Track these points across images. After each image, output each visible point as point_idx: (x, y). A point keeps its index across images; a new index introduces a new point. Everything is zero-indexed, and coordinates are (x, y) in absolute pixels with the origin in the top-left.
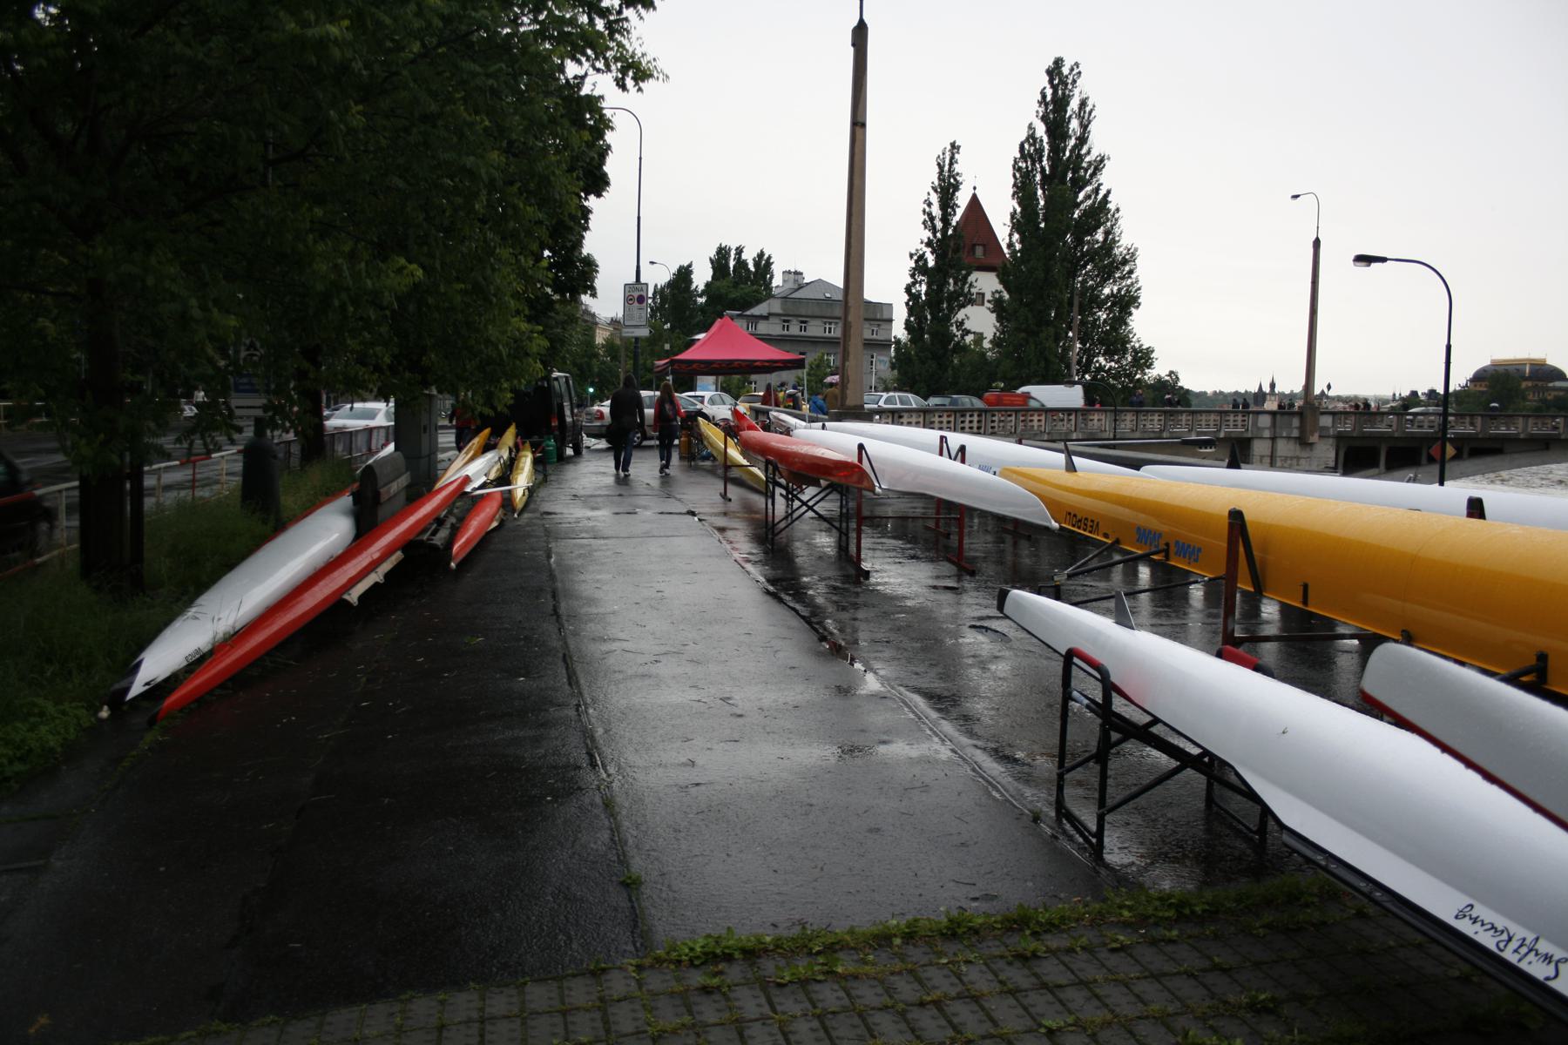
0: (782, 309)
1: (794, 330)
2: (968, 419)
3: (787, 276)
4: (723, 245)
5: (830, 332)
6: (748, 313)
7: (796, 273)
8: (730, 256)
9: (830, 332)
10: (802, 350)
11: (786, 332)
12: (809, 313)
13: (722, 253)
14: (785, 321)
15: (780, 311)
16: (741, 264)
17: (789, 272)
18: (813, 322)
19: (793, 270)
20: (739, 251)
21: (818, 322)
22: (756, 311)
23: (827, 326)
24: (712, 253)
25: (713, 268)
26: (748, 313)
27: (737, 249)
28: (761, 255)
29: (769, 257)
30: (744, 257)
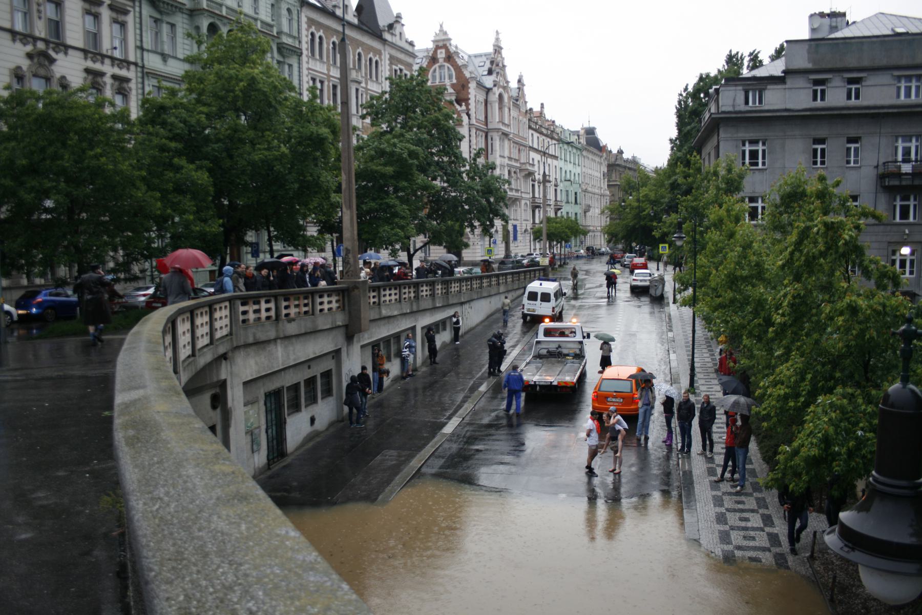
0: (810, 60)
1: (836, 96)
3: (818, 22)
4: (733, 53)
5: (908, 95)
7: (833, 15)
8: (742, 64)
9: (908, 95)
10: (853, 133)
11: (819, 103)
12: (866, 63)
14: (817, 82)
15: (809, 66)
17: (822, 15)
18: (872, 80)
19: (827, 11)
21: (885, 78)
23: (903, 85)
27: (751, 54)
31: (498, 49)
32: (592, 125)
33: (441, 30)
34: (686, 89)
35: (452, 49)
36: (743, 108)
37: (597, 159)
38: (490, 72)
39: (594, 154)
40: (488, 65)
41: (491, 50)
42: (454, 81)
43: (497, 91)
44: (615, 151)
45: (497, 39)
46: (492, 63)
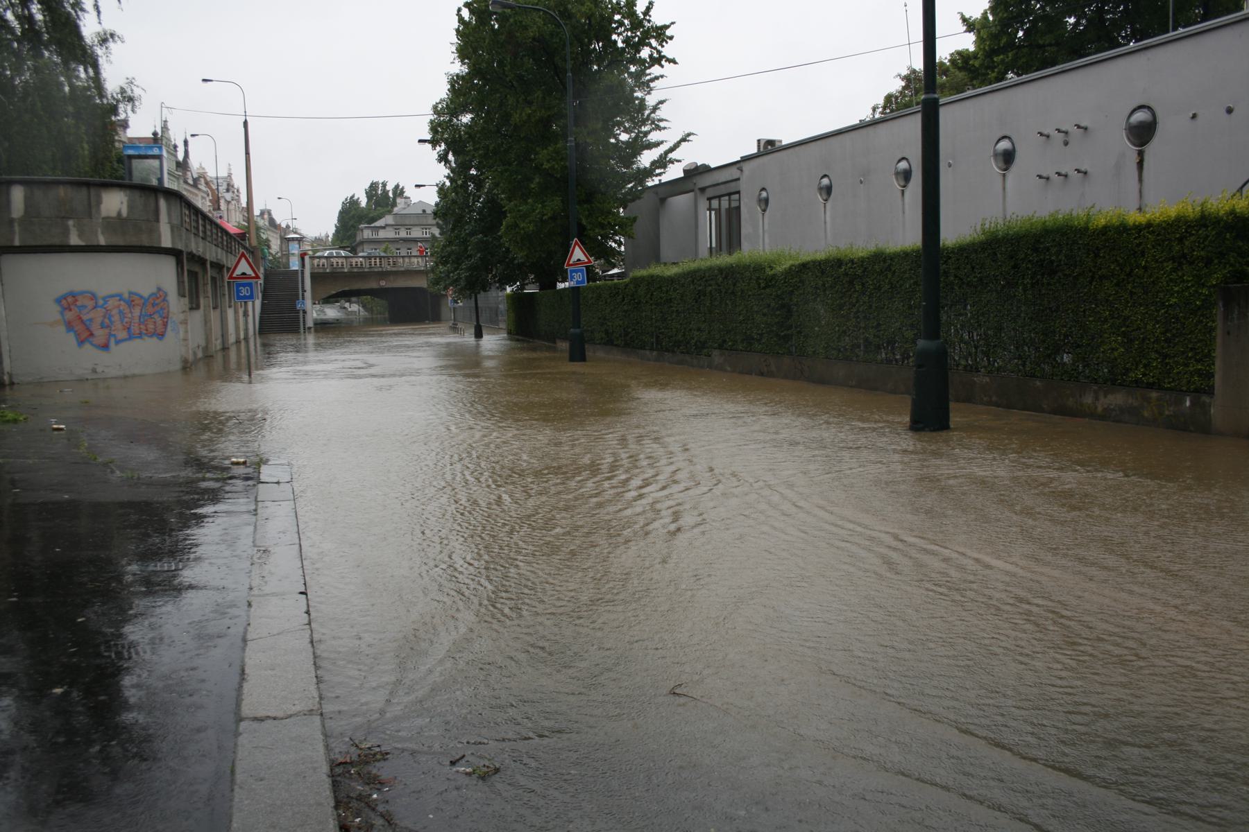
1: (403, 234)
2: (373, 260)
6: (373, 225)
12: (412, 223)
13: (374, 186)
15: (393, 223)
16: (385, 192)
18: (414, 229)
20: (384, 185)
21: (418, 228)
22: (377, 224)
24: (367, 186)
25: (367, 197)
26: (373, 225)
28: (397, 186)
29: (403, 188)
30: (388, 188)
31: (230, 175)
32: (268, 208)
33: (201, 167)
34: (346, 199)
35: (208, 179)
36: (371, 237)
37: (275, 236)
38: (228, 190)
39: (273, 231)
40: (225, 186)
41: (226, 175)
42: (211, 198)
43: (233, 202)
44: (284, 226)
45: (230, 169)
46: (228, 185)
